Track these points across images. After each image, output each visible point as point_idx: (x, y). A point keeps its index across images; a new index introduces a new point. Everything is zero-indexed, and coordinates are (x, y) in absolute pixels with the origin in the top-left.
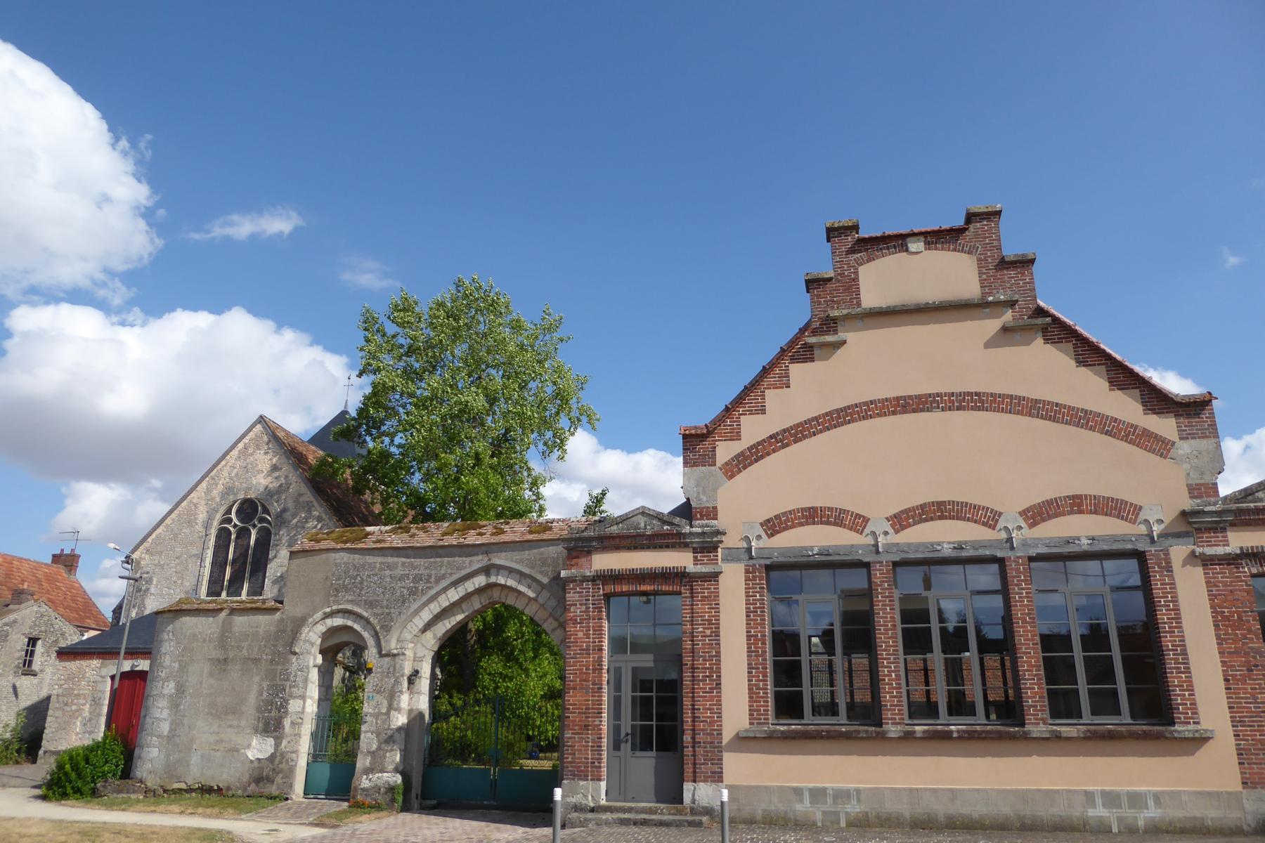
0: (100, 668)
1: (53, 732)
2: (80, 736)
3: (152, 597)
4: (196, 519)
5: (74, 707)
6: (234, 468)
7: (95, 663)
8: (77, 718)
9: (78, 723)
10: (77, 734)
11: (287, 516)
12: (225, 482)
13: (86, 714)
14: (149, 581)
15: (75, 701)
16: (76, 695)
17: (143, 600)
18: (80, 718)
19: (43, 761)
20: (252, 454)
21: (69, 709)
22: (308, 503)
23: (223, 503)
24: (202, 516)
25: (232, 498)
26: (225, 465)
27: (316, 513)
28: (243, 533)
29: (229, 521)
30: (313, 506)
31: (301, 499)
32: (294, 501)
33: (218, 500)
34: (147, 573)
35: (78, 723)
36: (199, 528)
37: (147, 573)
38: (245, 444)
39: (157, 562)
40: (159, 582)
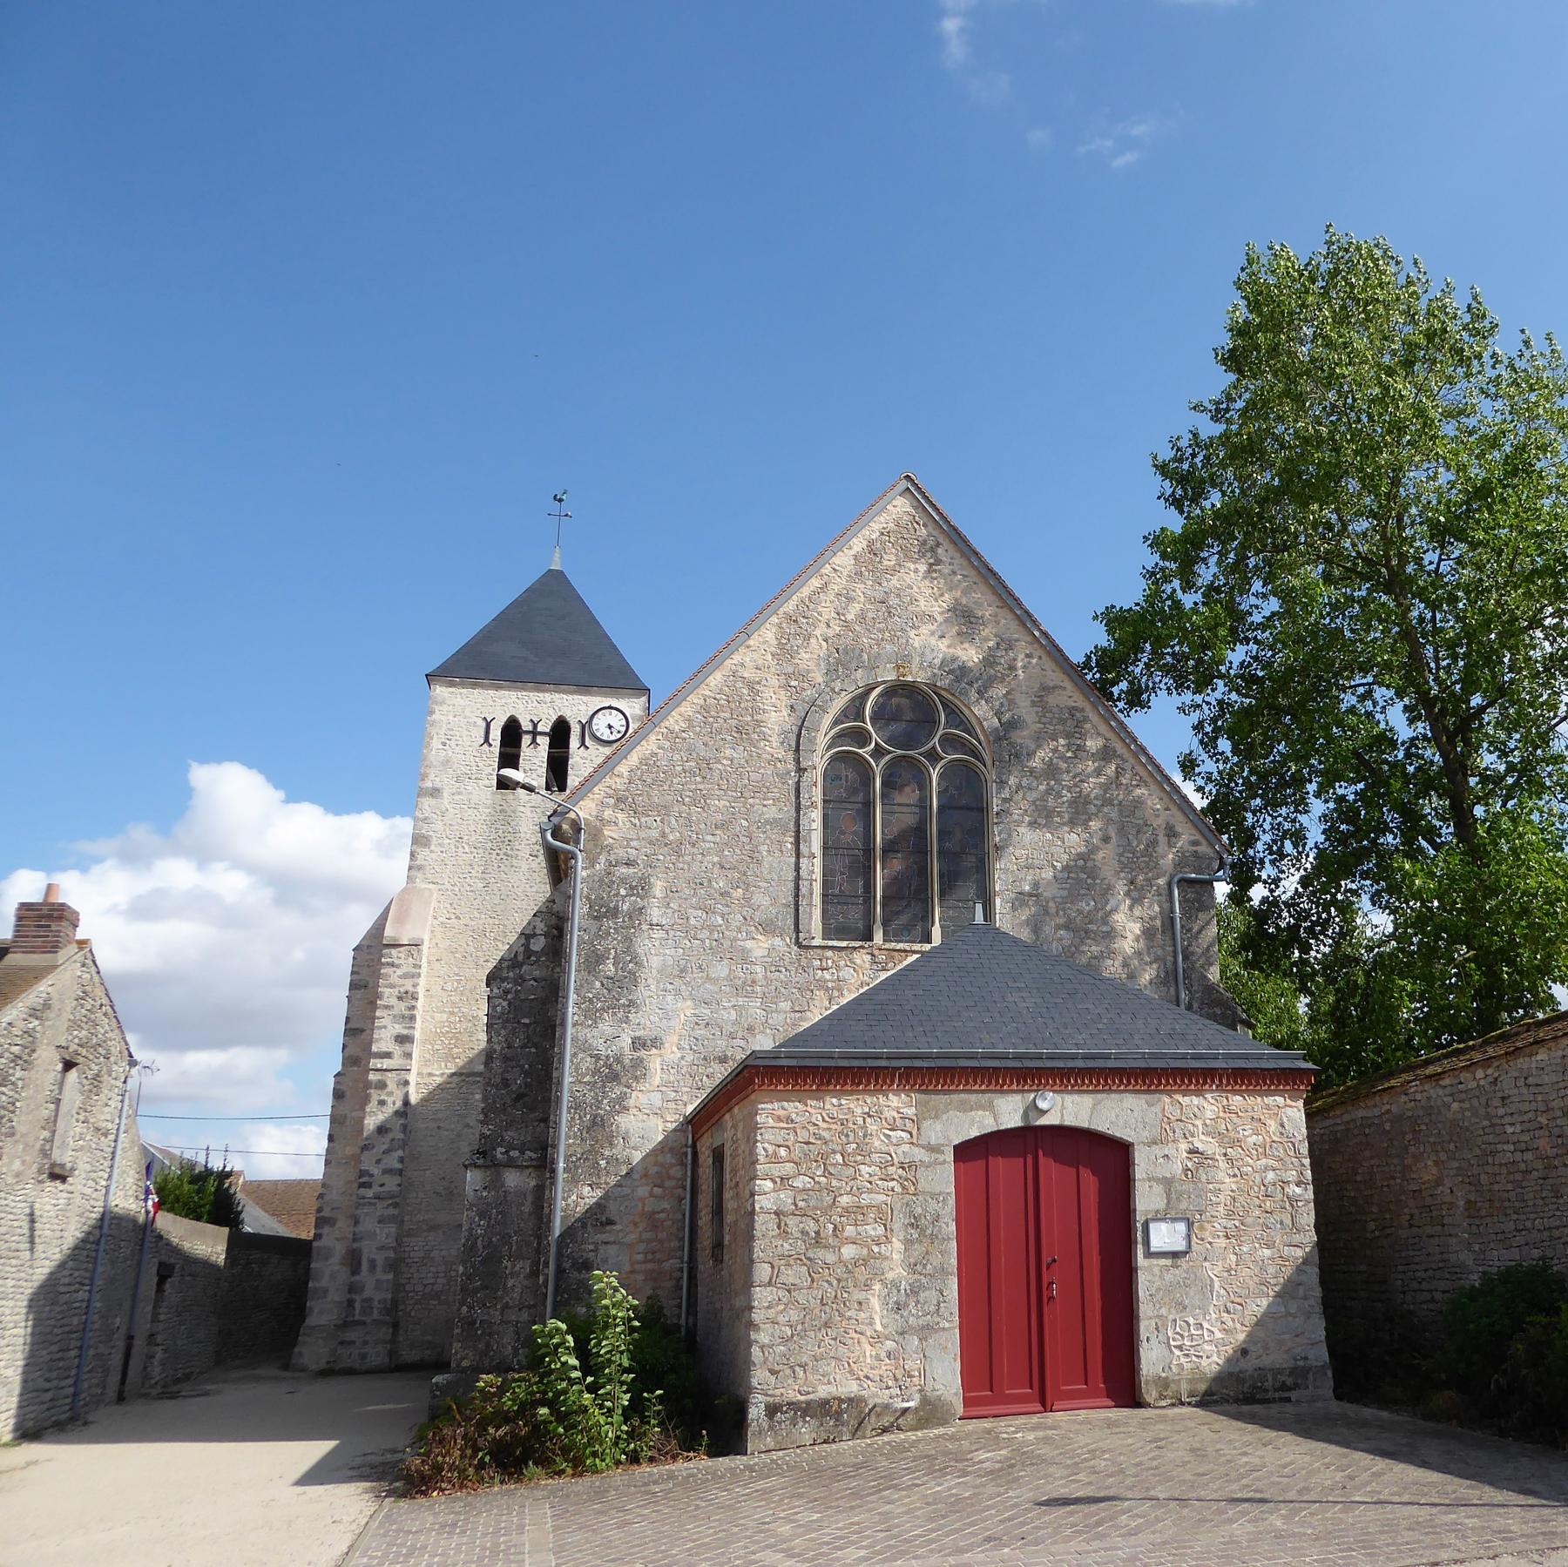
0: (918, 1121)
1: (786, 1340)
2: (890, 1345)
3: (658, 934)
4: (759, 723)
5: (848, 1252)
6: (850, 599)
7: (897, 1103)
8: (867, 1286)
9: (875, 1303)
10: (877, 1339)
11: (1022, 737)
12: (830, 633)
13: (897, 1271)
14: (641, 887)
15: (850, 1231)
16: (847, 1210)
17: (628, 940)
18: (877, 1287)
19: (769, 1442)
20: (894, 571)
21: (831, 1258)
22: (1072, 711)
23: (838, 686)
24: (777, 718)
25: (861, 678)
26: (824, 587)
27: (1093, 744)
28: (903, 773)
29: (861, 737)
30: (1086, 720)
31: (1052, 700)
32: (1034, 704)
33: (819, 678)
34: (629, 863)
35: (875, 1303)
36: (775, 748)
37: (629, 863)
38: (871, 543)
39: (655, 834)
40: (671, 891)
